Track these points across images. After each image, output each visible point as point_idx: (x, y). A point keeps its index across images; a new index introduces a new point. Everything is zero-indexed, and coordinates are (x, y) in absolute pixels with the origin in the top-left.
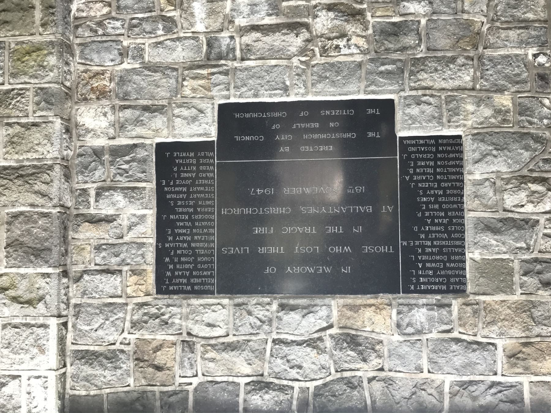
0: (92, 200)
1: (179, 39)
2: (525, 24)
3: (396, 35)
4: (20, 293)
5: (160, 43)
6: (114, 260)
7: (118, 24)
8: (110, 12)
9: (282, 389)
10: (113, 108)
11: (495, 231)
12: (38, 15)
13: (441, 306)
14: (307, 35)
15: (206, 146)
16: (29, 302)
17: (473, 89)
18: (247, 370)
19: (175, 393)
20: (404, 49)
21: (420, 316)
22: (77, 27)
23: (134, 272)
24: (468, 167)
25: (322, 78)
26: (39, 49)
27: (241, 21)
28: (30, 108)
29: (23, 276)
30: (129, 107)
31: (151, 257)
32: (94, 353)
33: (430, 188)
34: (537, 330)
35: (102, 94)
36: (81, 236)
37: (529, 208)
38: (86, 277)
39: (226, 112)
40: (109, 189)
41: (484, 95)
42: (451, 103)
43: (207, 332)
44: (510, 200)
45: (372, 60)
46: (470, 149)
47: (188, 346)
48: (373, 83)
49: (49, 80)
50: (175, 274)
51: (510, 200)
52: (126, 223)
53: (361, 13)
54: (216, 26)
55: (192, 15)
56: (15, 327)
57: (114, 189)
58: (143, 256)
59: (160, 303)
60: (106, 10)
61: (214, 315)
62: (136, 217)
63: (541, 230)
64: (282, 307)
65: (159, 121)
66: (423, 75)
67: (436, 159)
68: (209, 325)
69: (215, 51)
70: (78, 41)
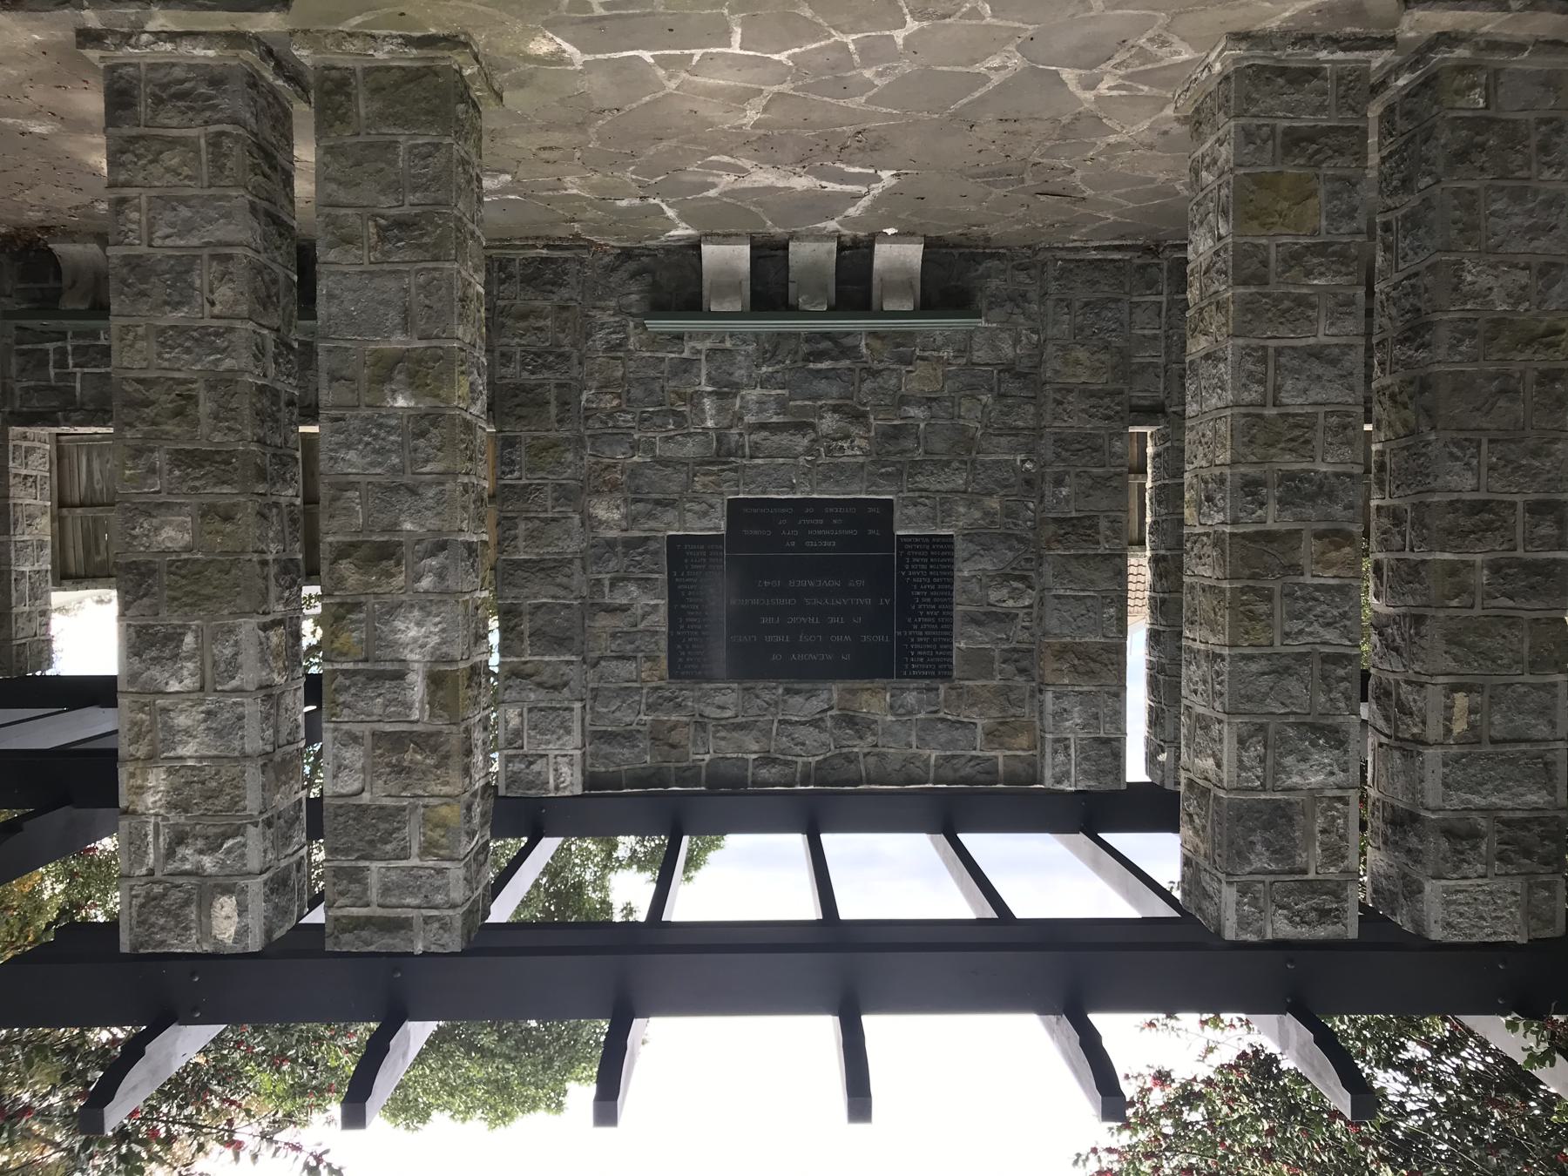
0: (607, 590)
1: (689, 435)
2: (1015, 431)
3: (896, 438)
4: (544, 678)
5: (671, 437)
6: (629, 647)
7: (629, 417)
8: (619, 405)
9: (787, 763)
10: (625, 500)
11: (979, 623)
12: (553, 410)
13: (929, 690)
14: (813, 436)
15: (716, 539)
16: (554, 688)
17: (965, 492)
18: (755, 747)
19: (689, 768)
20: (903, 452)
21: (911, 698)
22: (587, 418)
23: (648, 658)
24: (958, 565)
25: (826, 478)
26: (555, 445)
27: (750, 419)
28: (549, 503)
29: (548, 663)
30: (640, 501)
31: (664, 644)
32: (611, 733)
33: (924, 583)
34: (1012, 711)
35: (614, 487)
36: (597, 624)
37: (1010, 603)
38: (603, 663)
39: (735, 507)
40: (623, 579)
41: (976, 497)
42: (943, 506)
43: (717, 713)
44: (994, 596)
45: (873, 462)
46: (961, 548)
47: (701, 725)
48: (874, 484)
49: (566, 476)
50: (685, 661)
51: (994, 596)
52: (640, 612)
53: (864, 415)
54: (726, 422)
55: (703, 411)
56: (541, 710)
57: (628, 579)
58: (656, 643)
59: (673, 687)
60: (615, 403)
61: (724, 699)
62: (649, 605)
63: (1020, 623)
64: (787, 691)
65: (670, 515)
66: (919, 478)
67: (929, 556)
68: (719, 707)
69: (724, 448)
70: (589, 432)
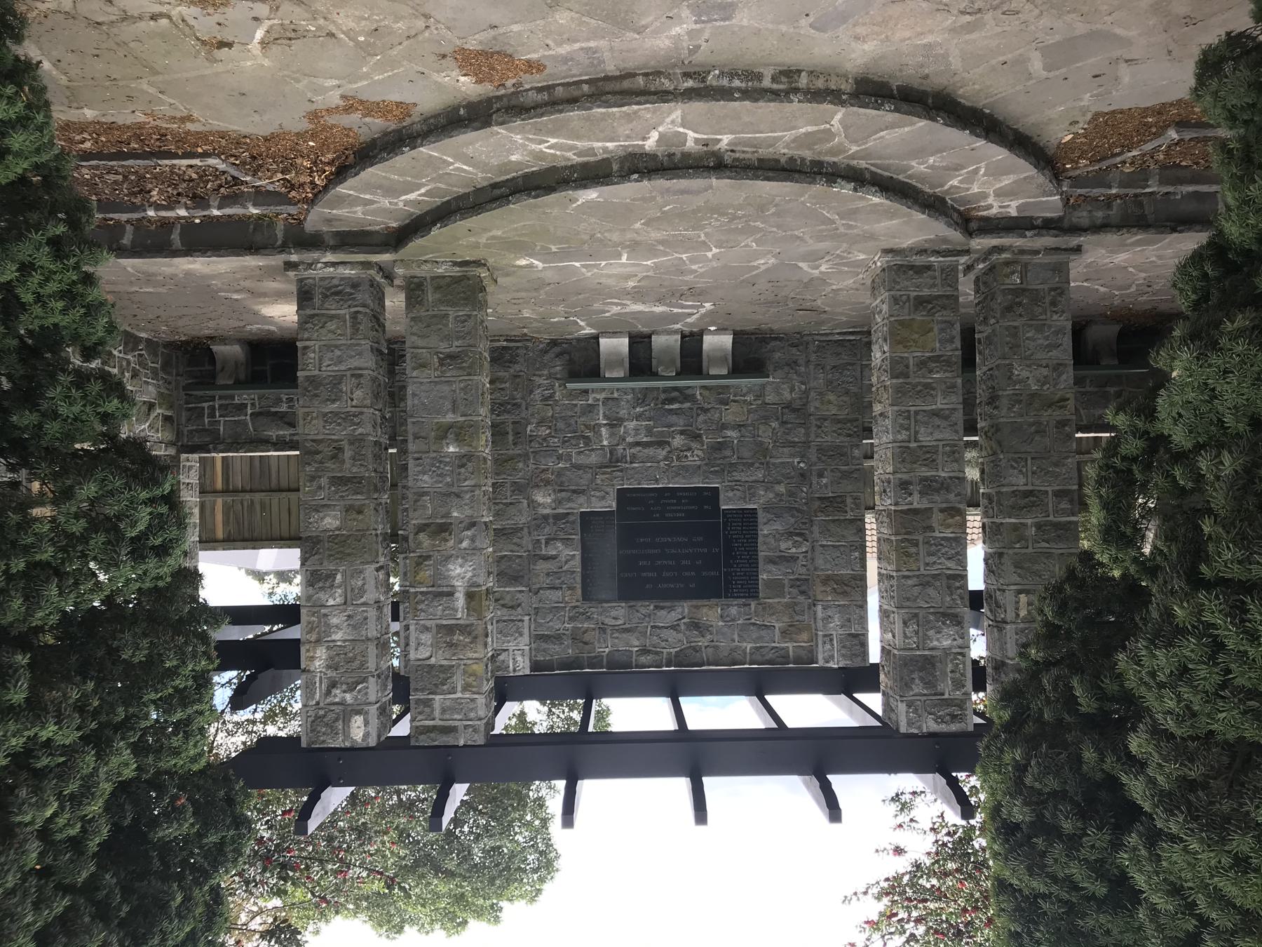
2: (793, 444)
9: (657, 653)
11: (774, 563)
12: (511, 438)
13: (745, 605)
16: (512, 607)
18: (637, 643)
20: (725, 457)
21: (734, 611)
23: (569, 588)
24: (760, 527)
28: (509, 494)
31: (579, 579)
34: (797, 618)
35: (548, 483)
37: (794, 550)
39: (622, 493)
42: (750, 490)
43: (613, 622)
44: (783, 546)
46: (762, 517)
49: (518, 477)
51: (783, 546)
53: (700, 436)
54: (615, 442)
61: (618, 613)
62: (569, 554)
64: (656, 607)
65: (582, 499)
